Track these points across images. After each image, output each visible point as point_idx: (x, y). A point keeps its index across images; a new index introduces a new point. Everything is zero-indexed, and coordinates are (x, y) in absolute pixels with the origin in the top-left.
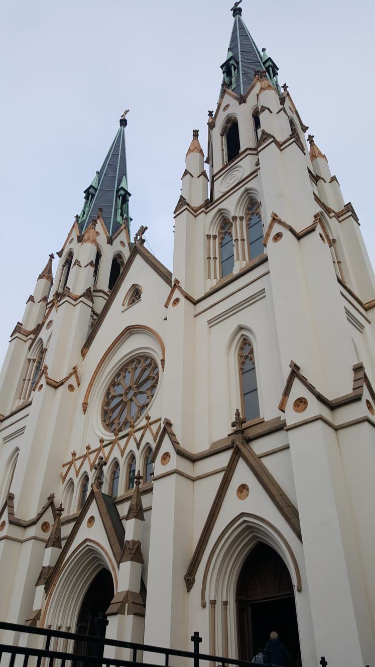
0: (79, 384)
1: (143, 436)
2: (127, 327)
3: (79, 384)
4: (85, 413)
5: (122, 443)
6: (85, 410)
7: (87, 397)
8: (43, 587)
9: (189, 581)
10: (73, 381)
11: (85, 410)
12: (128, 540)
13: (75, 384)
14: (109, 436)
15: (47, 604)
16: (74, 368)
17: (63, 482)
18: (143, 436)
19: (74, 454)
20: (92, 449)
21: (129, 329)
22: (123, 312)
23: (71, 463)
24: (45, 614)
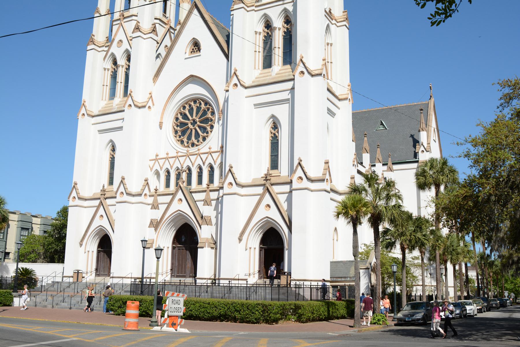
0: (154, 105)
1: (207, 158)
2: (191, 75)
3: (154, 105)
4: (161, 129)
5: (193, 158)
6: (161, 127)
7: (162, 118)
8: (153, 229)
9: (240, 240)
10: (150, 104)
11: (161, 127)
12: (206, 215)
13: (151, 106)
14: (183, 150)
15: (157, 237)
16: (150, 94)
17: (151, 171)
18: (207, 158)
19: (157, 155)
20: (170, 156)
21: (193, 77)
22: (185, 59)
23: (156, 160)
24: (156, 241)
